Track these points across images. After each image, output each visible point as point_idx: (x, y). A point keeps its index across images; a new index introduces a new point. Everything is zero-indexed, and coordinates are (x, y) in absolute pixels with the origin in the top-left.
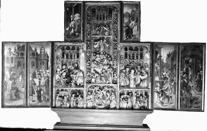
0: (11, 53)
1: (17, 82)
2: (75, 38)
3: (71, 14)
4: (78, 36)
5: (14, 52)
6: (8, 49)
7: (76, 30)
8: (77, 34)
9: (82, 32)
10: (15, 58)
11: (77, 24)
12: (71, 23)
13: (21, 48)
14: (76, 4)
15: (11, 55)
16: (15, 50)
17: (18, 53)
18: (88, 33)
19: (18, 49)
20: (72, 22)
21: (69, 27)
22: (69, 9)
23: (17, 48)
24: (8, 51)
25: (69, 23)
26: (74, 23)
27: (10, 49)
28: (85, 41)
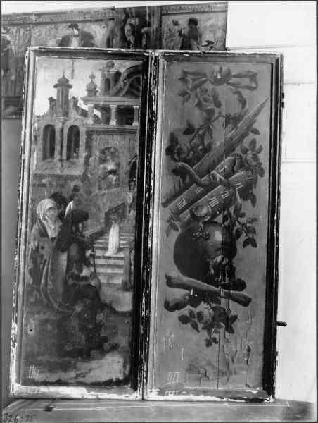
0: (71, 104)
1: (93, 256)
5: (86, 101)
6: (55, 86)
10: (89, 134)
13: (122, 78)
15: (66, 114)
16: (92, 91)
17: (106, 110)
19: (107, 83)
23: (99, 82)
24: (54, 93)
27: (63, 85)
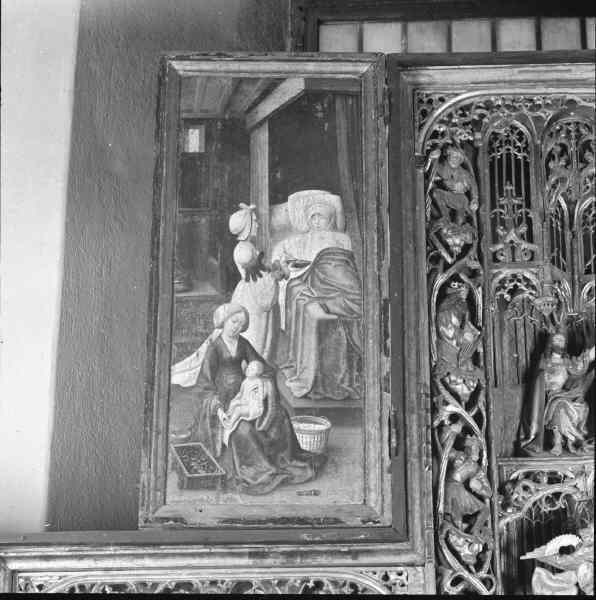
2: (284, 483)
3: (238, 194)
4: (321, 462)
7: (295, 387)
8: (309, 434)
9: (372, 412)
11: (316, 312)
12: (227, 298)
14: (293, 88)
18: (454, 418)
20: (241, 285)
21: (204, 348)
22: (208, 138)
25: (200, 301)
26: (275, 307)
28: (420, 522)
